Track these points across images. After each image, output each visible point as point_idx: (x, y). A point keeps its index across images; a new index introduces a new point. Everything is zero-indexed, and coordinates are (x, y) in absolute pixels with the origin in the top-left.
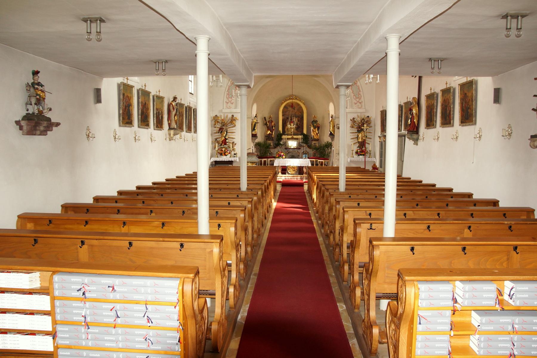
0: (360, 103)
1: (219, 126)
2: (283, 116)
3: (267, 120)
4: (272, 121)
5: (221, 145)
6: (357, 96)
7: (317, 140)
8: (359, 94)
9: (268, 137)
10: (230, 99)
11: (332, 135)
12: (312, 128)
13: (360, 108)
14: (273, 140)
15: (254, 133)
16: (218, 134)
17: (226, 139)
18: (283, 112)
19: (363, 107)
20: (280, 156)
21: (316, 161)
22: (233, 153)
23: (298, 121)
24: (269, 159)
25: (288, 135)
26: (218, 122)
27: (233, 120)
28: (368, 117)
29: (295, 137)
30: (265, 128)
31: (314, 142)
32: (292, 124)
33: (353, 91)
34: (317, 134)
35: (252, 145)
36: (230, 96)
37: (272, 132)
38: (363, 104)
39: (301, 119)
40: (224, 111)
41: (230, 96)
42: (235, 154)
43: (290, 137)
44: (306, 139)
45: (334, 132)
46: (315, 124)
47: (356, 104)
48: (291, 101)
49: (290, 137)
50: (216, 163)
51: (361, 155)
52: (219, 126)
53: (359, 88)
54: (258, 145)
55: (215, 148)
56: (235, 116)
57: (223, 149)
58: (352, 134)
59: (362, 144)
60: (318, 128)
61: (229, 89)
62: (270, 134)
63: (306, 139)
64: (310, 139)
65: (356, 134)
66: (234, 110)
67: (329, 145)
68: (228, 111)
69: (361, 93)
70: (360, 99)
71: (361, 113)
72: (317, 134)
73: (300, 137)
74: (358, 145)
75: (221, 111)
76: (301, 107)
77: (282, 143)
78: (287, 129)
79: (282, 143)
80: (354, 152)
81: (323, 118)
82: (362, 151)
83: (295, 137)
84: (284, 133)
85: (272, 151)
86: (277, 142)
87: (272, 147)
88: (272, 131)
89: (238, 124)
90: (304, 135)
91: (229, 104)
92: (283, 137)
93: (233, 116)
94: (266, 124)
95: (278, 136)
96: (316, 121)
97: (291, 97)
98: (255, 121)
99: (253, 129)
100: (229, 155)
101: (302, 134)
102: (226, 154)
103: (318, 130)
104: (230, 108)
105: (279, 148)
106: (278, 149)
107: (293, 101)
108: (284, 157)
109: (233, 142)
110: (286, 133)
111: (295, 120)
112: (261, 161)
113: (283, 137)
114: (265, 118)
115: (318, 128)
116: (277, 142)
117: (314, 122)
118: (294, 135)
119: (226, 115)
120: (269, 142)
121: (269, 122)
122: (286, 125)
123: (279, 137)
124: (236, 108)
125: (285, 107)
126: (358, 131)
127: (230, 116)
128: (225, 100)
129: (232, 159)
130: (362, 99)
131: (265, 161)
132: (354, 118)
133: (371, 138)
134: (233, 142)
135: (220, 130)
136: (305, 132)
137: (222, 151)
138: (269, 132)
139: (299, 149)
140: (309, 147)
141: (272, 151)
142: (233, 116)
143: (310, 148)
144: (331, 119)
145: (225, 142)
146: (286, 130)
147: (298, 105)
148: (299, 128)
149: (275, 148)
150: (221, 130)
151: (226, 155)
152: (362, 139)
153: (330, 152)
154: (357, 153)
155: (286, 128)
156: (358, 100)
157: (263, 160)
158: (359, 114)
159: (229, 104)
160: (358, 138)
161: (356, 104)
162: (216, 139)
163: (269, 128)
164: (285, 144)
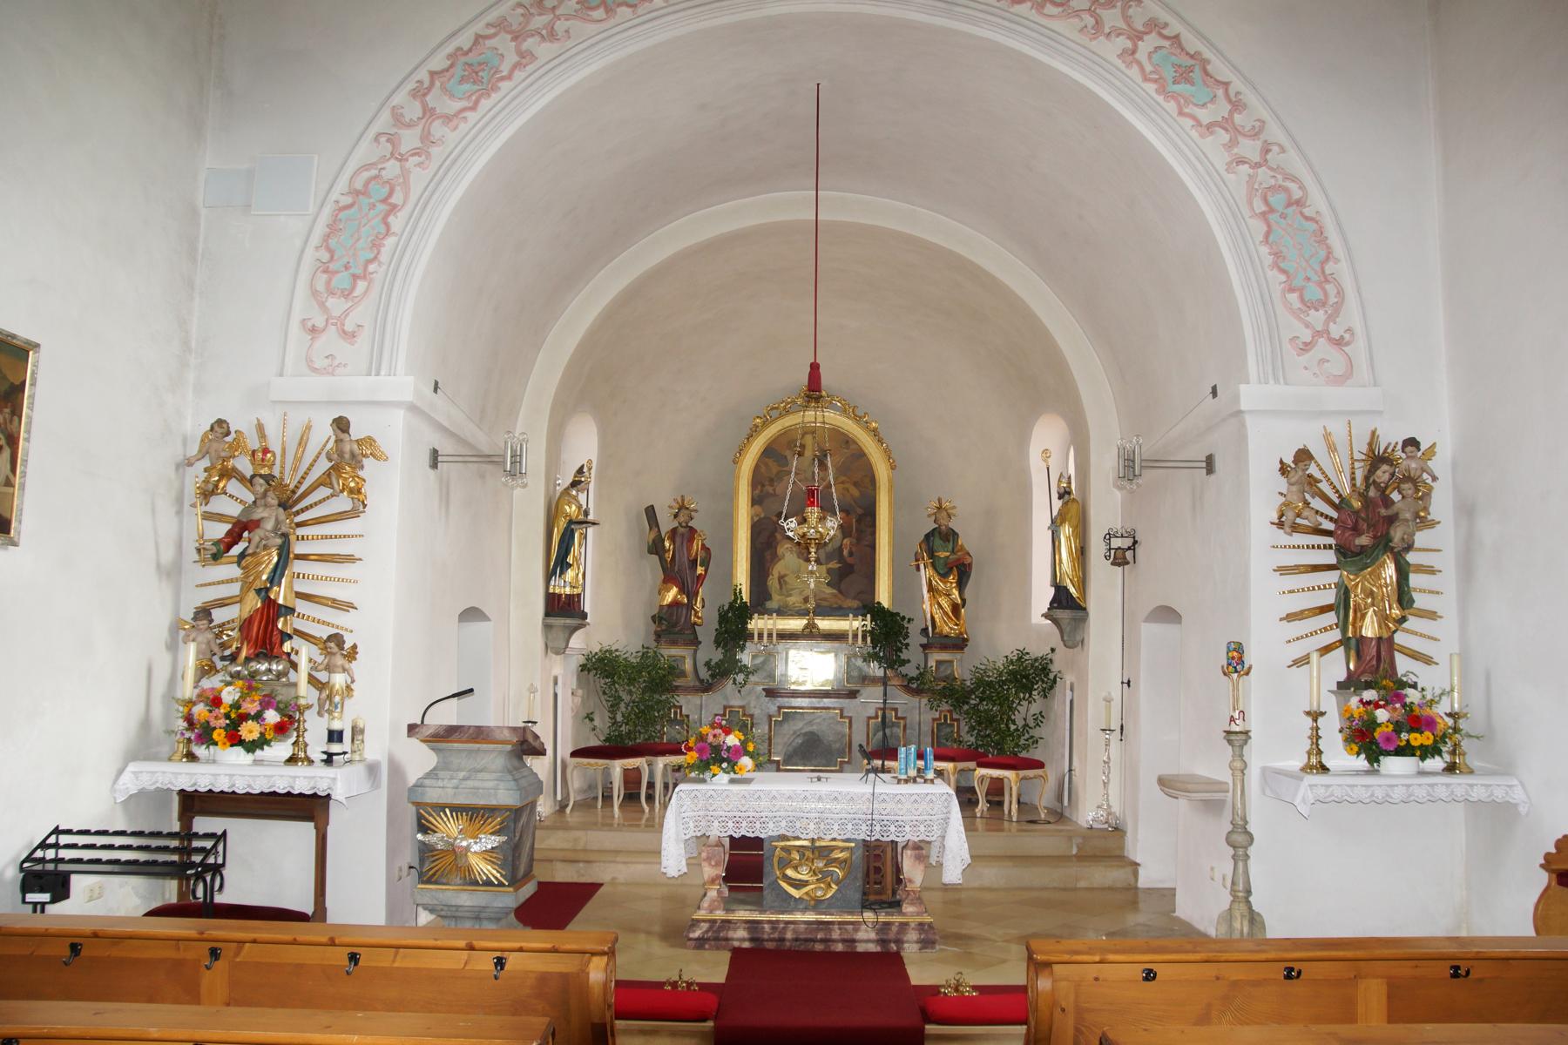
0: (1339, 343)
2: (755, 501)
3: (666, 523)
6: (1313, 292)
9: (671, 624)
10: (336, 305)
11: (1067, 604)
12: (925, 574)
13: (1340, 380)
15: (561, 587)
16: (229, 570)
18: (757, 481)
20: (715, 758)
22: (315, 729)
24: (661, 762)
25: (782, 612)
26: (227, 473)
27: (347, 459)
28: (1412, 443)
29: (824, 624)
31: (935, 657)
32: (813, 513)
33: (1277, 255)
34: (956, 609)
35: (564, 670)
36: (342, 280)
37: (692, 595)
38: (1358, 349)
39: (861, 521)
41: (342, 280)
42: (335, 736)
43: (797, 624)
44: (888, 632)
45: (1083, 584)
49: (797, 624)
50: (194, 803)
51: (1405, 751)
52: (235, 510)
53: (1320, 236)
54: (602, 668)
56: (356, 432)
57: (229, 695)
59: (1373, 668)
61: (333, 228)
62: (675, 604)
63: (888, 632)
65: (1332, 577)
67: (1031, 676)
68: (314, 387)
70: (1331, 318)
74: (1337, 666)
76: (861, 455)
78: (781, 578)
79: (745, 658)
82: (1416, 721)
83: (824, 624)
84: (761, 600)
85: (688, 704)
86: (717, 655)
87: (690, 680)
89: (392, 486)
90: (877, 612)
91: (330, 341)
92: (756, 624)
93: (341, 425)
94: (656, 548)
95: (723, 618)
96: (949, 536)
98: (571, 510)
99: (559, 563)
100: (281, 749)
102: (249, 731)
103: (961, 586)
104: (330, 371)
105: (729, 686)
108: (746, 761)
109: (337, 639)
112: (607, 773)
114: (651, 512)
116: (717, 655)
119: (297, 420)
120: (675, 651)
121: (673, 533)
122: (775, 558)
123: (733, 627)
124: (374, 369)
125: (769, 452)
126: (1343, 551)
127: (323, 433)
128: (302, 306)
129: (301, 781)
130: (1352, 315)
131: (632, 778)
132: (1303, 456)
133: (1432, 615)
135: (234, 537)
136: (884, 597)
137: (216, 702)
138: (672, 594)
139: (853, 694)
140: (916, 686)
141: (688, 704)
142: (341, 425)
143: (918, 692)
145: (265, 633)
146: (773, 582)
147: (846, 441)
148: (851, 572)
149: (705, 688)
151: (251, 747)
152: (1383, 618)
153: (1040, 719)
155: (778, 569)
156: (1317, 317)
157: (618, 767)
158: (1338, 429)
161: (1307, 347)
162: (204, 613)
163: (671, 575)
164: (766, 664)
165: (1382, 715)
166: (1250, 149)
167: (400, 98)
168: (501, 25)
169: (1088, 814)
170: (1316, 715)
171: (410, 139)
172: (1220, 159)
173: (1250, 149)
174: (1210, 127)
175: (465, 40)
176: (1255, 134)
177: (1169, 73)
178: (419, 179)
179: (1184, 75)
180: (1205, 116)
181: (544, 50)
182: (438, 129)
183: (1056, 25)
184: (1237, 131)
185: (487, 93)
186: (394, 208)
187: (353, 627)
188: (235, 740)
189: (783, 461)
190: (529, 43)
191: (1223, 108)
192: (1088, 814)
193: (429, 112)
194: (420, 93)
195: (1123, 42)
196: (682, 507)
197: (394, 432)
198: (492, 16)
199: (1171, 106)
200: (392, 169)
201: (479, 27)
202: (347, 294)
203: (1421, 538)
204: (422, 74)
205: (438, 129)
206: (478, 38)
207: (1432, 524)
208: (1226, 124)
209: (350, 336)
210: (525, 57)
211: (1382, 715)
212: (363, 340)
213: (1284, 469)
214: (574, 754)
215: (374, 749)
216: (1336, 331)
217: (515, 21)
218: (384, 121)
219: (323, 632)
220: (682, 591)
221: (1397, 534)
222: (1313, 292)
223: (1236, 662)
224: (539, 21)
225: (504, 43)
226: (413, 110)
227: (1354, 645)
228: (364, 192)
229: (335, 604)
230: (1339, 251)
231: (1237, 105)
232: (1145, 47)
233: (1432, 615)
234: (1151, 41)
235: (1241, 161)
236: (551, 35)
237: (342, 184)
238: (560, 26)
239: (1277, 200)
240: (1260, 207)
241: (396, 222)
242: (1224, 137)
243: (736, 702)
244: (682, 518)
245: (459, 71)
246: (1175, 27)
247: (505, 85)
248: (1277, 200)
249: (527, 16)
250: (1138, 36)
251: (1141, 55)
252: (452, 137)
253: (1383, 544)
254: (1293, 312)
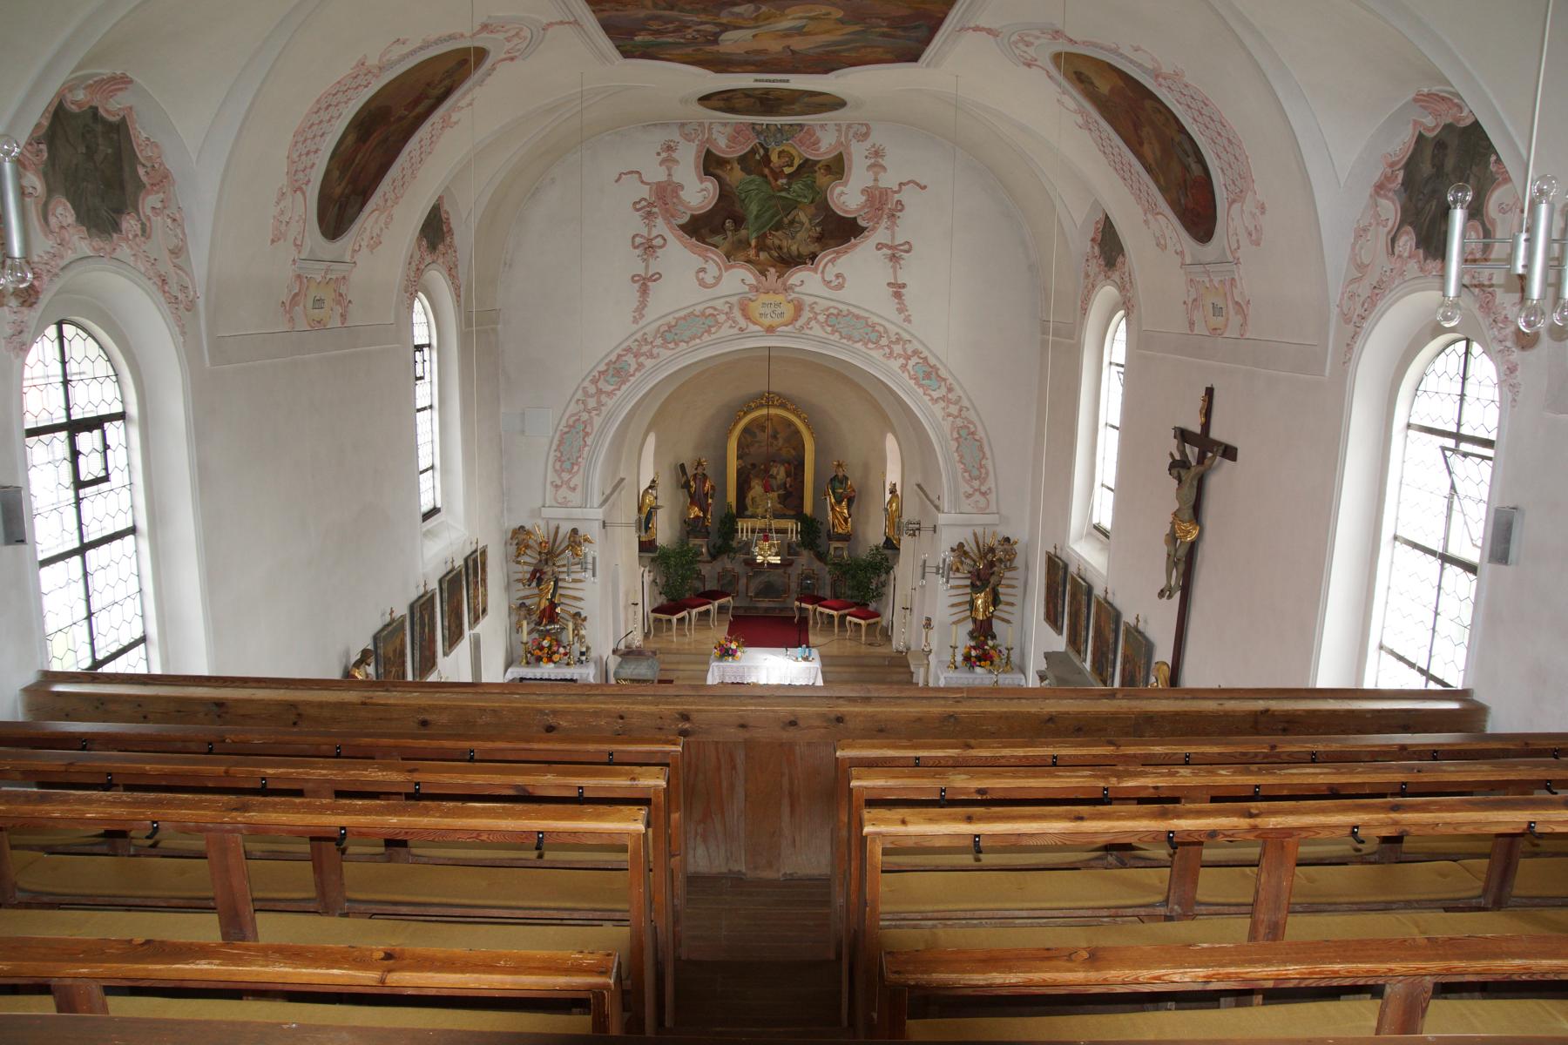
0: (984, 494)
1: (531, 558)
3: (690, 472)
4: (705, 477)
5: (539, 624)
6: (975, 473)
7: (846, 538)
8: (981, 466)
9: (691, 528)
10: (566, 476)
11: (891, 545)
13: (983, 512)
14: (707, 534)
17: (553, 605)
19: (993, 508)
21: (843, 617)
23: (788, 474)
26: (527, 547)
30: (682, 496)
33: (961, 457)
36: (567, 465)
37: (705, 512)
38: (992, 497)
39: (797, 467)
40: (546, 513)
41: (567, 465)
44: (812, 532)
46: (842, 487)
47: (969, 496)
48: (764, 411)
53: (981, 448)
55: (519, 629)
56: (581, 532)
57: (546, 643)
58: (954, 592)
60: (850, 501)
62: (697, 517)
64: (824, 535)
66: (577, 513)
69: (988, 463)
70: (983, 480)
71: (984, 526)
72: (846, 520)
73: (790, 525)
74: (970, 626)
75: (536, 513)
76: (797, 432)
77: (734, 544)
80: (959, 658)
81: (866, 467)
84: (742, 510)
86: (719, 542)
87: (706, 557)
88: (705, 512)
91: (564, 491)
92: (741, 524)
93: (575, 531)
94: (686, 485)
97: (767, 399)
101: (799, 515)
102: (556, 657)
104: (564, 504)
106: (726, 563)
107: (773, 411)
109: (578, 614)
110: (748, 513)
111: (780, 472)
113: (741, 524)
114: (682, 466)
115: (850, 501)
116: (719, 542)
117: (838, 481)
118: (776, 516)
119: (553, 525)
120: (698, 541)
121: (695, 476)
122: (750, 488)
125: (746, 430)
127: (566, 528)
128: (551, 476)
130: (991, 483)
132: (961, 545)
133: (1012, 604)
134: (578, 614)
135: (533, 574)
136: (808, 508)
137: (541, 648)
144: (888, 496)
145: (550, 614)
146: (748, 501)
147: (790, 424)
148: (791, 499)
150: (537, 576)
153: (884, 584)
154: (967, 658)
156: (976, 484)
158: (979, 531)
159: (564, 491)
160: (972, 603)
161: (969, 496)
164: (747, 547)
165: (973, 653)
166: (954, 409)
167: (587, 383)
168: (628, 350)
169: (898, 643)
170: (954, 648)
171: (592, 403)
172: (939, 414)
173: (954, 409)
174: (936, 401)
175: (613, 357)
176: (956, 403)
177: (921, 375)
178: (597, 421)
179: (928, 376)
180: (935, 395)
181: (649, 363)
182: (604, 398)
183: (873, 353)
184: (949, 402)
185: (624, 382)
186: (587, 434)
187: (586, 608)
188: (550, 660)
189: (754, 435)
190: (642, 359)
191: (943, 391)
192: (898, 643)
193: (600, 391)
194: (595, 381)
195: (902, 361)
196: (699, 464)
197: (592, 530)
198: (625, 345)
199: (920, 391)
200: (585, 416)
201: (619, 351)
202: (570, 471)
203: (1008, 574)
204: (595, 373)
205: (604, 398)
206: (619, 356)
207: (1015, 569)
208: (943, 398)
209: (574, 489)
210: (641, 366)
211: (973, 653)
212: (579, 489)
213: (953, 550)
214: (654, 611)
215: (593, 654)
216: (983, 489)
217: (634, 346)
218: (579, 395)
219: (573, 611)
220: (701, 509)
221: (993, 580)
222: (975, 473)
223: (928, 624)
224: (645, 349)
225: (630, 359)
226: (592, 389)
227: (975, 620)
228: (573, 426)
229: (575, 598)
230: (988, 454)
231: (950, 390)
232: (911, 363)
233: (1012, 604)
234: (914, 360)
235: (949, 415)
236: (651, 356)
237: (563, 423)
238: (655, 351)
239: (964, 433)
240: (955, 435)
241: (589, 440)
242: (942, 404)
243: (729, 566)
244: (700, 470)
245: (611, 372)
246: (926, 353)
247: (632, 379)
248: (964, 433)
249: (640, 346)
250: (908, 358)
251: (910, 367)
252: (610, 403)
253: (985, 583)
254: (967, 482)
